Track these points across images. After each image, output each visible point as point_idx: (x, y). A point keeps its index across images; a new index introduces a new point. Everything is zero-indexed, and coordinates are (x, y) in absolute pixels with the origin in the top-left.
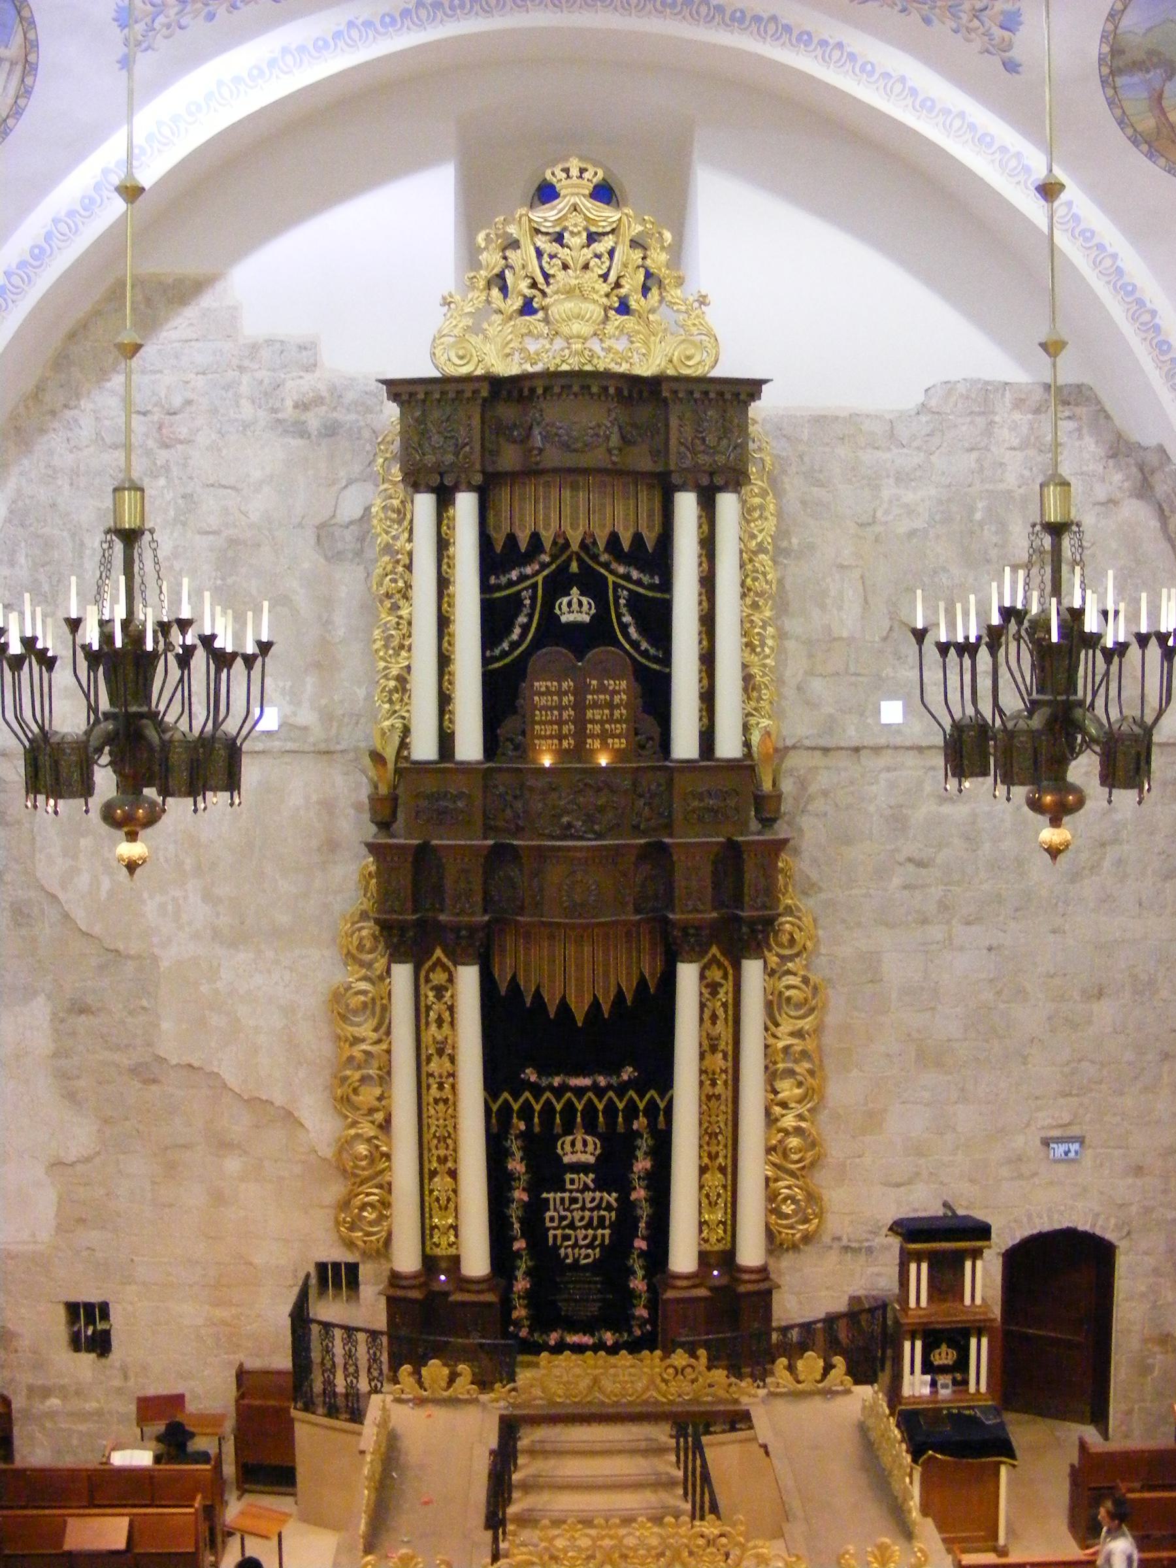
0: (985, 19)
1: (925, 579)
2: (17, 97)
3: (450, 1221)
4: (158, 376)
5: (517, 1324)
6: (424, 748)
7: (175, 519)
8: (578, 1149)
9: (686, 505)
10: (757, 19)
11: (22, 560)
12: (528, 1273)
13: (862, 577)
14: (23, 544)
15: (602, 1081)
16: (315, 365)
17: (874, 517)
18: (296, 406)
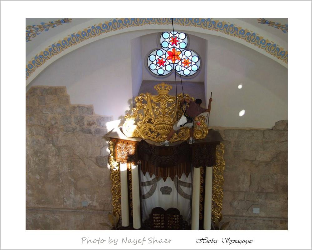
1: (269, 177)
4: (47, 115)
7: (55, 154)
13: (250, 176)
16: (92, 113)
17: (256, 159)
18: (88, 124)
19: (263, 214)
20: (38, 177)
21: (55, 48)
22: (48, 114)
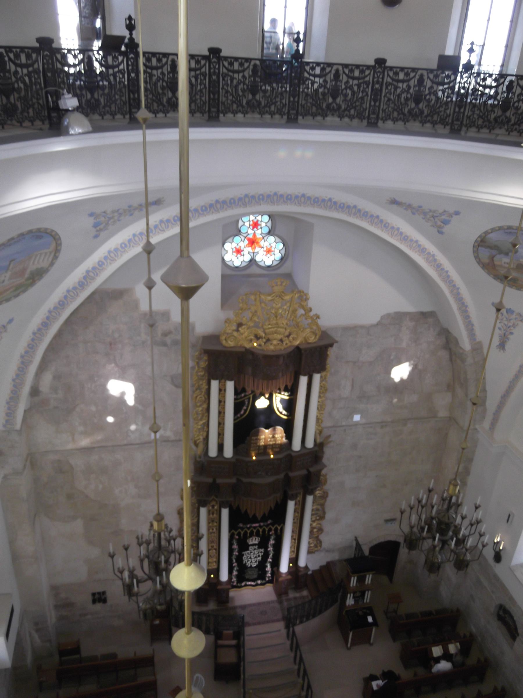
0: (436, 219)
3: (215, 560)
5: (233, 582)
6: (213, 452)
8: (254, 541)
9: (303, 380)
10: (349, 207)
12: (237, 571)
15: (262, 524)
19: (364, 421)
20: (93, 408)
21: (137, 239)
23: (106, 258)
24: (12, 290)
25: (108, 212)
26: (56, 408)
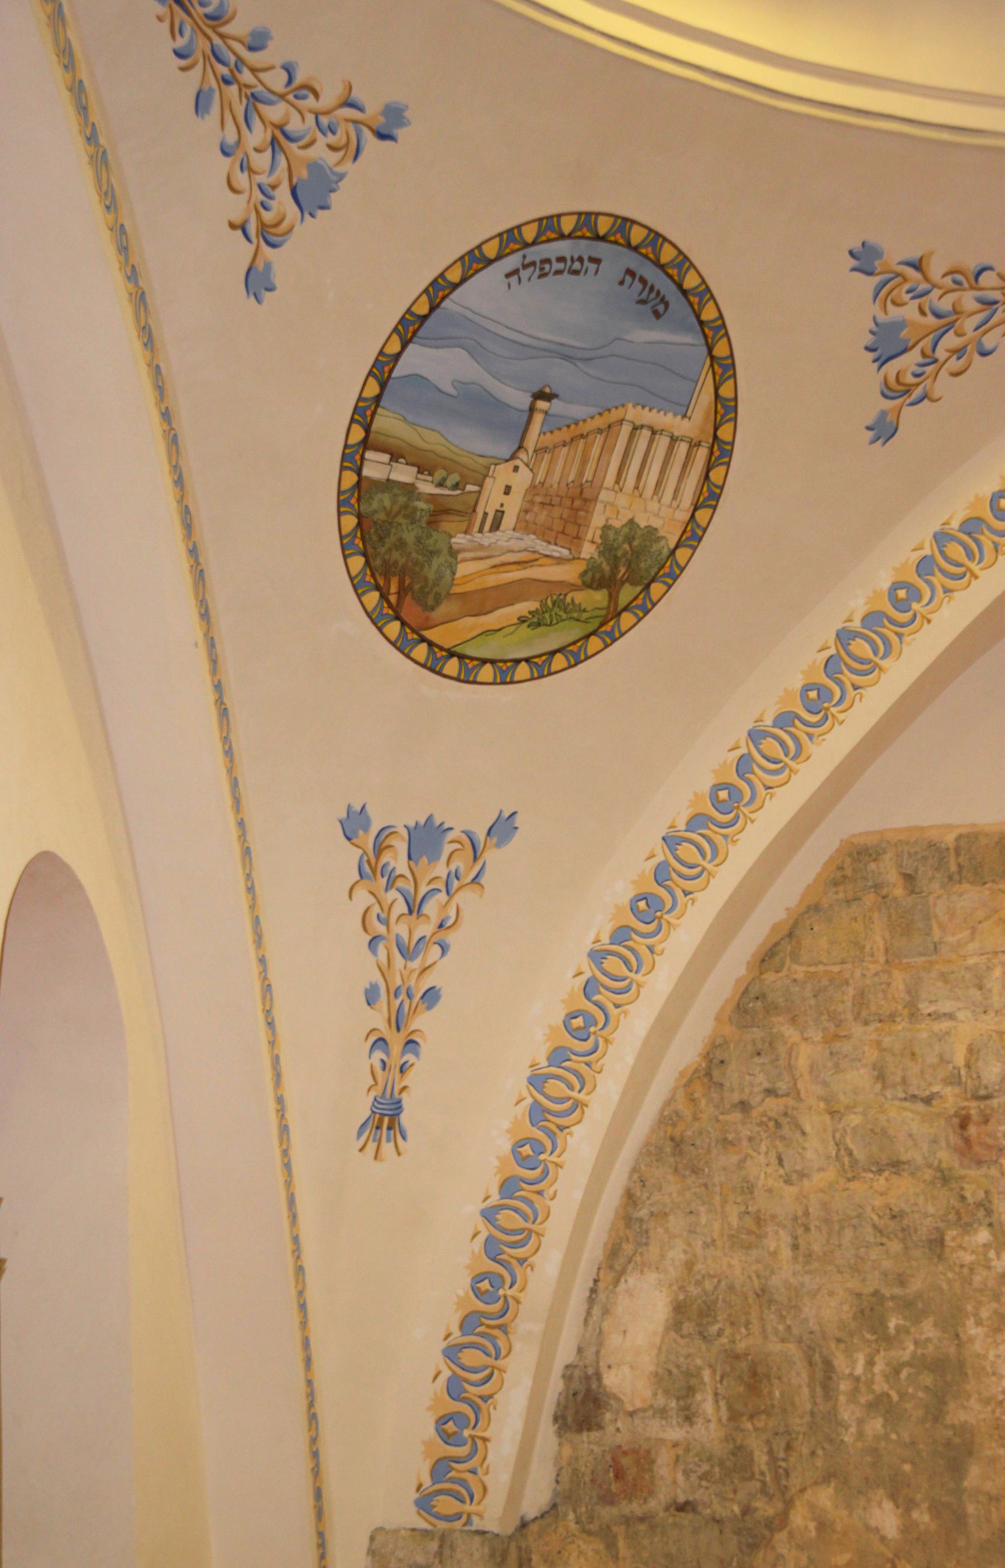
2: (695, 509)
4: (945, 1025)
11: (708, 1407)
14: (706, 1375)
20: (886, 1518)
22: (951, 1016)
23: (924, 566)
24: (524, 608)
25: (936, 270)
26: (682, 1508)
